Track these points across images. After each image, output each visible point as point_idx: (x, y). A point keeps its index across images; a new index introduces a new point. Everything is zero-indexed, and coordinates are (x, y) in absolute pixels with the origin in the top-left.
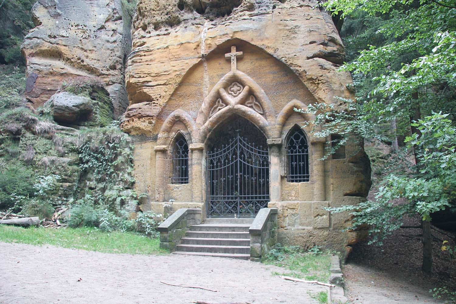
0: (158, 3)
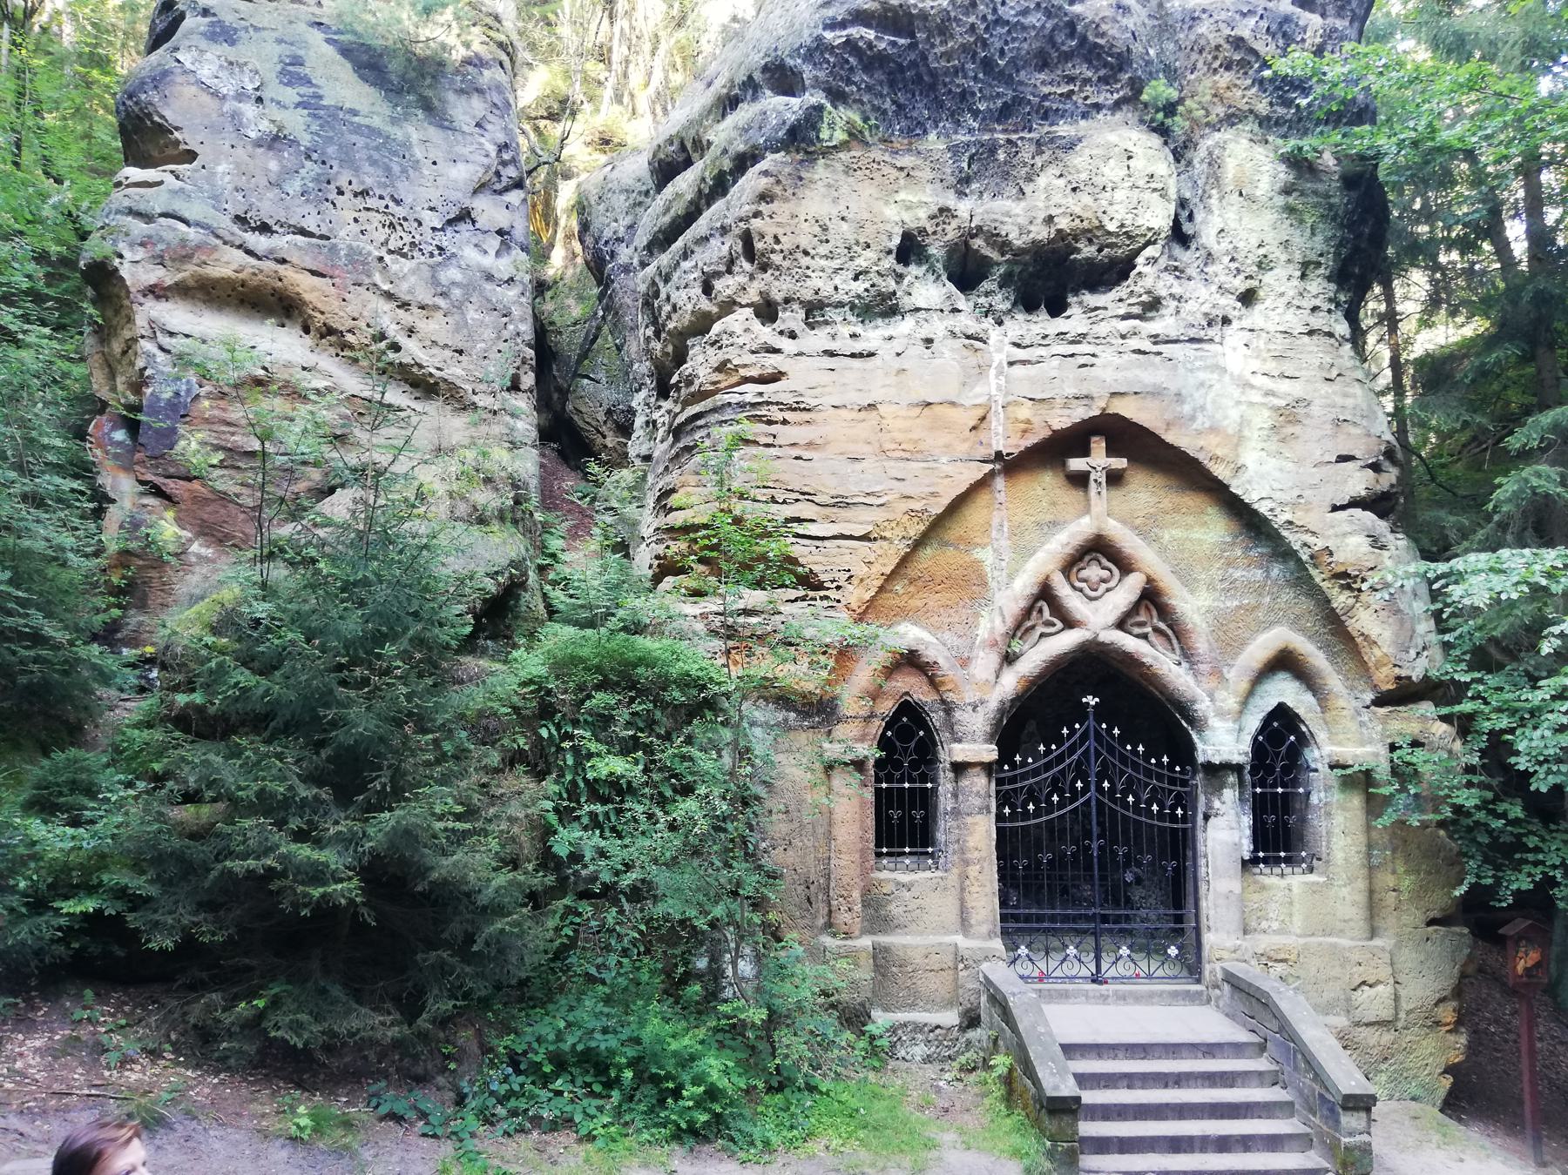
0: (825, 229)
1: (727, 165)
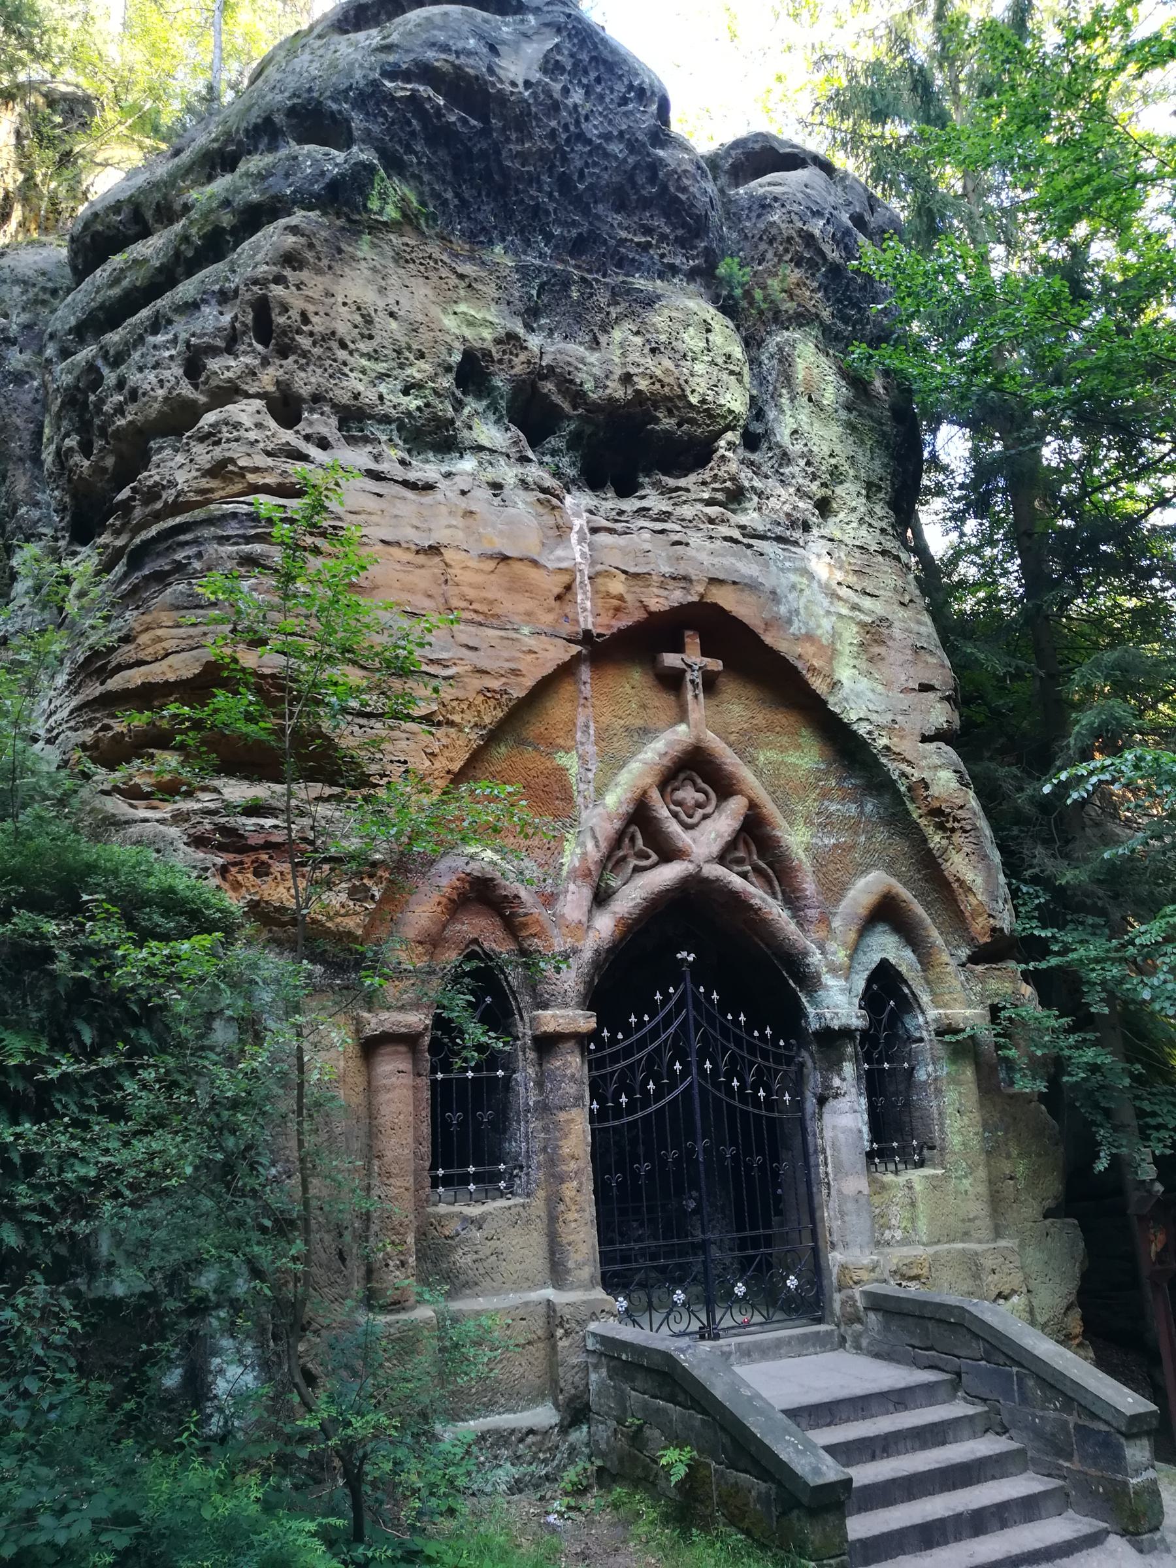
0: (368, 321)
1: (227, 219)
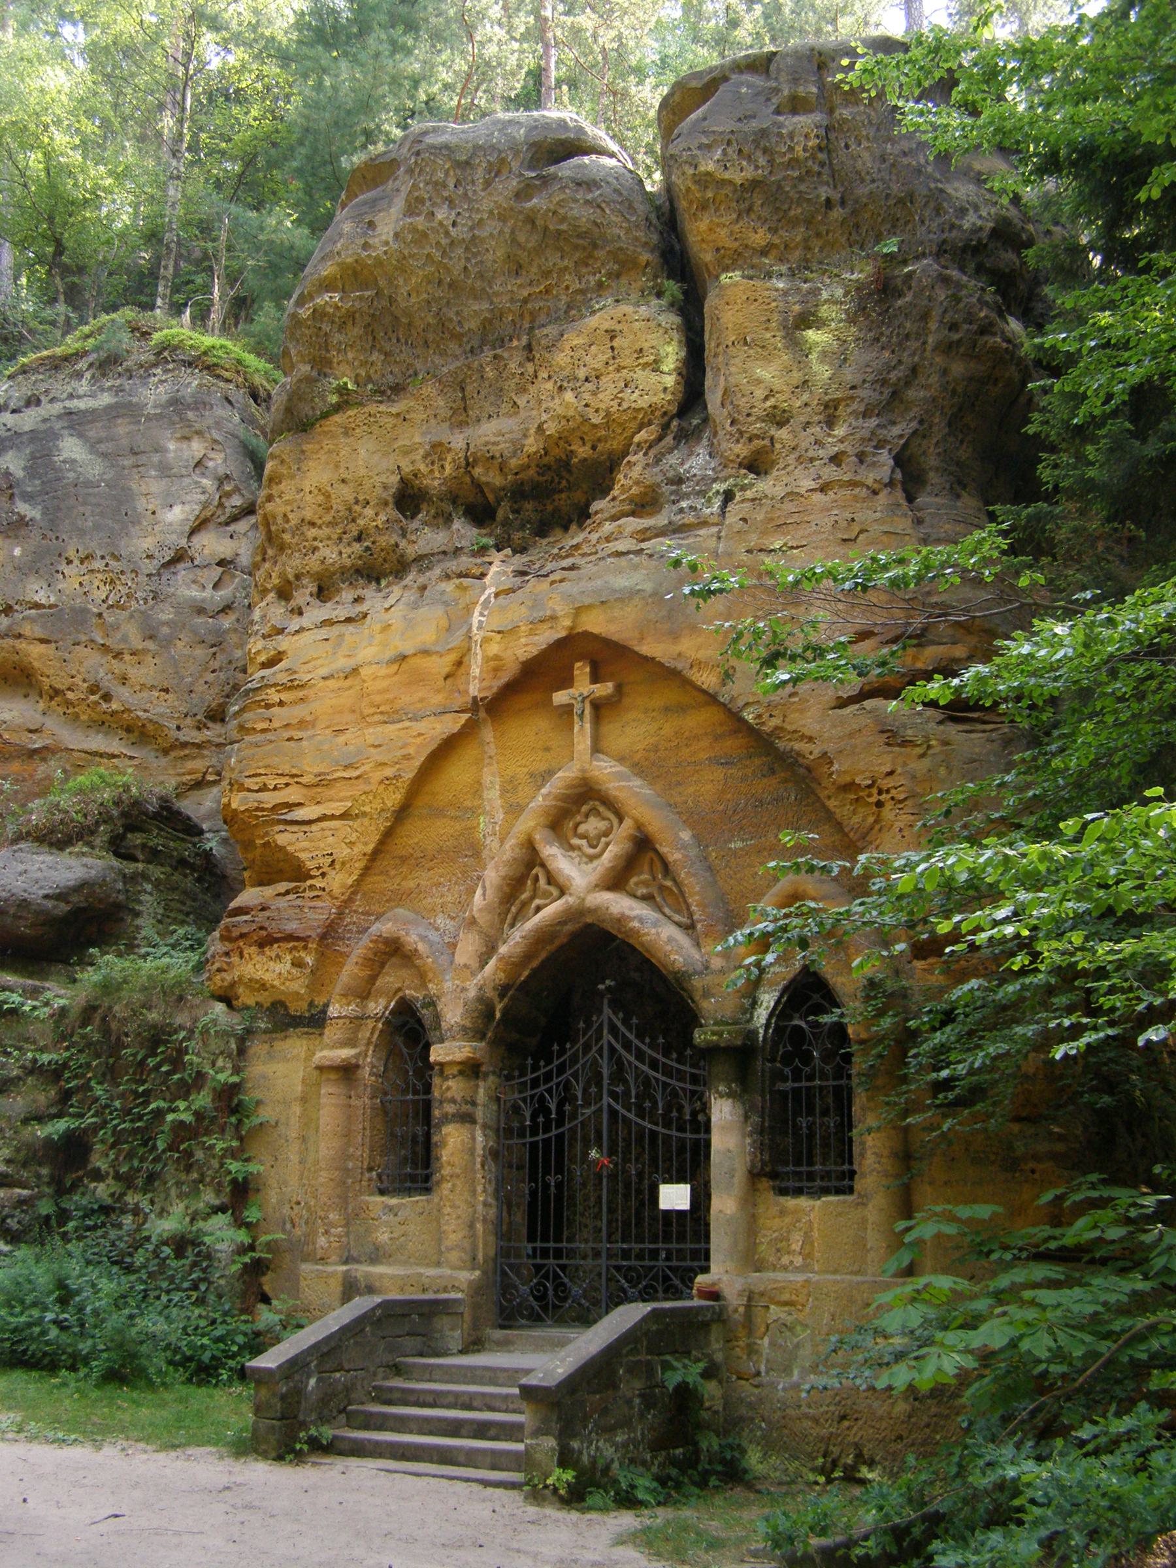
0: (328, 496)
